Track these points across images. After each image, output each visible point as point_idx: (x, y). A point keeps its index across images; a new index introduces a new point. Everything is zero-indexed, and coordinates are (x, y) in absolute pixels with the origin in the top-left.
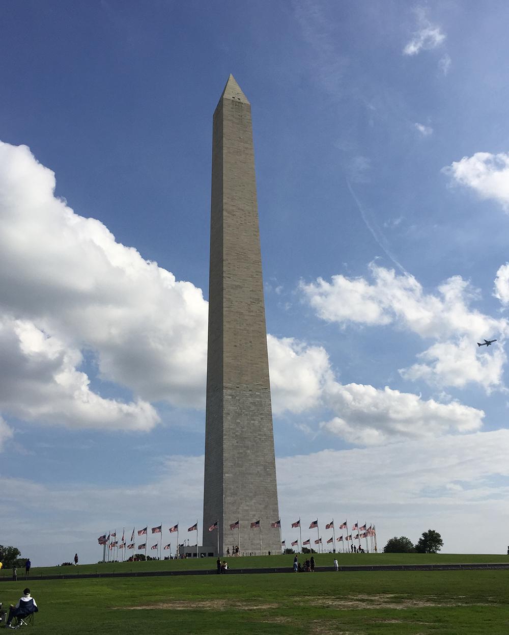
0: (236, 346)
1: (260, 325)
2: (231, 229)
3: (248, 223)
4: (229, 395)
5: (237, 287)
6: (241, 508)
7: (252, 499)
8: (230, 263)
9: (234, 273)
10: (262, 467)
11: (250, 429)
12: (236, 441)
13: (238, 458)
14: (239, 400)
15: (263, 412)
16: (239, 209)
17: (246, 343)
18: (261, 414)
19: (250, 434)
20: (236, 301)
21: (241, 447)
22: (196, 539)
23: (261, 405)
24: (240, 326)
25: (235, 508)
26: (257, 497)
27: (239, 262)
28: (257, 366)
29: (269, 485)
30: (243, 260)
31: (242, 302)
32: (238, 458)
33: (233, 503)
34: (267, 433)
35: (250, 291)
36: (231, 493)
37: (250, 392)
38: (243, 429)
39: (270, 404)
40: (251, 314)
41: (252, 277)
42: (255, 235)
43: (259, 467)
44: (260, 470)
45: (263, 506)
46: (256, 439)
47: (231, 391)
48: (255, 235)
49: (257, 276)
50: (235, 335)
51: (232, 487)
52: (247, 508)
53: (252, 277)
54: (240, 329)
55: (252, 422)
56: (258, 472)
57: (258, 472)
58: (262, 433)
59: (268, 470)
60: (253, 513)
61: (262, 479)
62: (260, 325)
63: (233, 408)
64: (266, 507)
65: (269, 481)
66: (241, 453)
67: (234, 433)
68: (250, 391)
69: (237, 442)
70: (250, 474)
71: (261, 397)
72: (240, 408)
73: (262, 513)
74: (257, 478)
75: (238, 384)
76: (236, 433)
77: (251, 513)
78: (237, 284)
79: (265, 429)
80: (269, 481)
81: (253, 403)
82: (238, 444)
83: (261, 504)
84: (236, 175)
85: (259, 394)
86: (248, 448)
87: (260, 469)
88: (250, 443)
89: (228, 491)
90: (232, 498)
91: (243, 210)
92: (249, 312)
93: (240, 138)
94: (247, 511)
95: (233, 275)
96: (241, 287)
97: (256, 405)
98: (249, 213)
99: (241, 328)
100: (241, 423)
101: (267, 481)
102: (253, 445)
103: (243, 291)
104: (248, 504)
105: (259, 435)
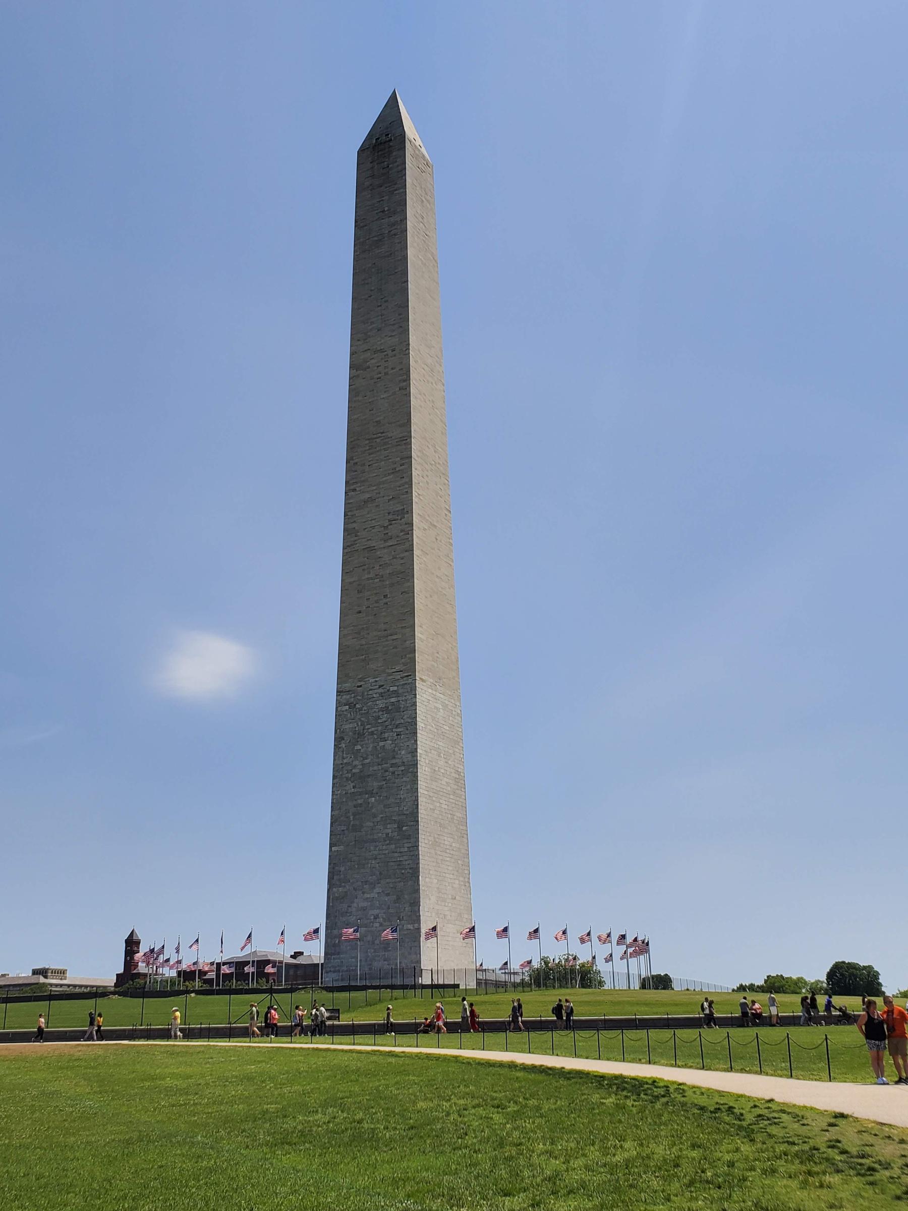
0: (360, 612)
1: (402, 559)
2: (360, 398)
6: (355, 905)
7: (374, 888)
11: (378, 757)
12: (352, 785)
14: (361, 709)
15: (402, 721)
16: (375, 352)
21: (361, 794)
23: (398, 710)
25: (345, 906)
28: (395, 637)
32: (354, 815)
34: (405, 760)
35: (389, 500)
37: (381, 690)
38: (367, 761)
39: (415, 704)
40: (390, 543)
41: (394, 471)
43: (389, 826)
47: (348, 697)
52: (365, 904)
55: (381, 744)
57: (387, 834)
58: (397, 761)
59: (404, 828)
60: (376, 912)
61: (393, 846)
62: (402, 559)
63: (351, 725)
64: (398, 898)
65: (406, 849)
68: (380, 686)
70: (374, 841)
73: (391, 911)
77: (371, 912)
78: (367, 496)
79: (403, 752)
80: (406, 849)
83: (388, 895)
86: (371, 794)
87: (390, 829)
88: (375, 784)
89: (335, 877)
91: (382, 351)
93: (383, 211)
94: (364, 909)
95: (363, 481)
96: (371, 500)
99: (371, 576)
101: (402, 850)
102: (381, 787)
104: (368, 896)
105: (392, 765)
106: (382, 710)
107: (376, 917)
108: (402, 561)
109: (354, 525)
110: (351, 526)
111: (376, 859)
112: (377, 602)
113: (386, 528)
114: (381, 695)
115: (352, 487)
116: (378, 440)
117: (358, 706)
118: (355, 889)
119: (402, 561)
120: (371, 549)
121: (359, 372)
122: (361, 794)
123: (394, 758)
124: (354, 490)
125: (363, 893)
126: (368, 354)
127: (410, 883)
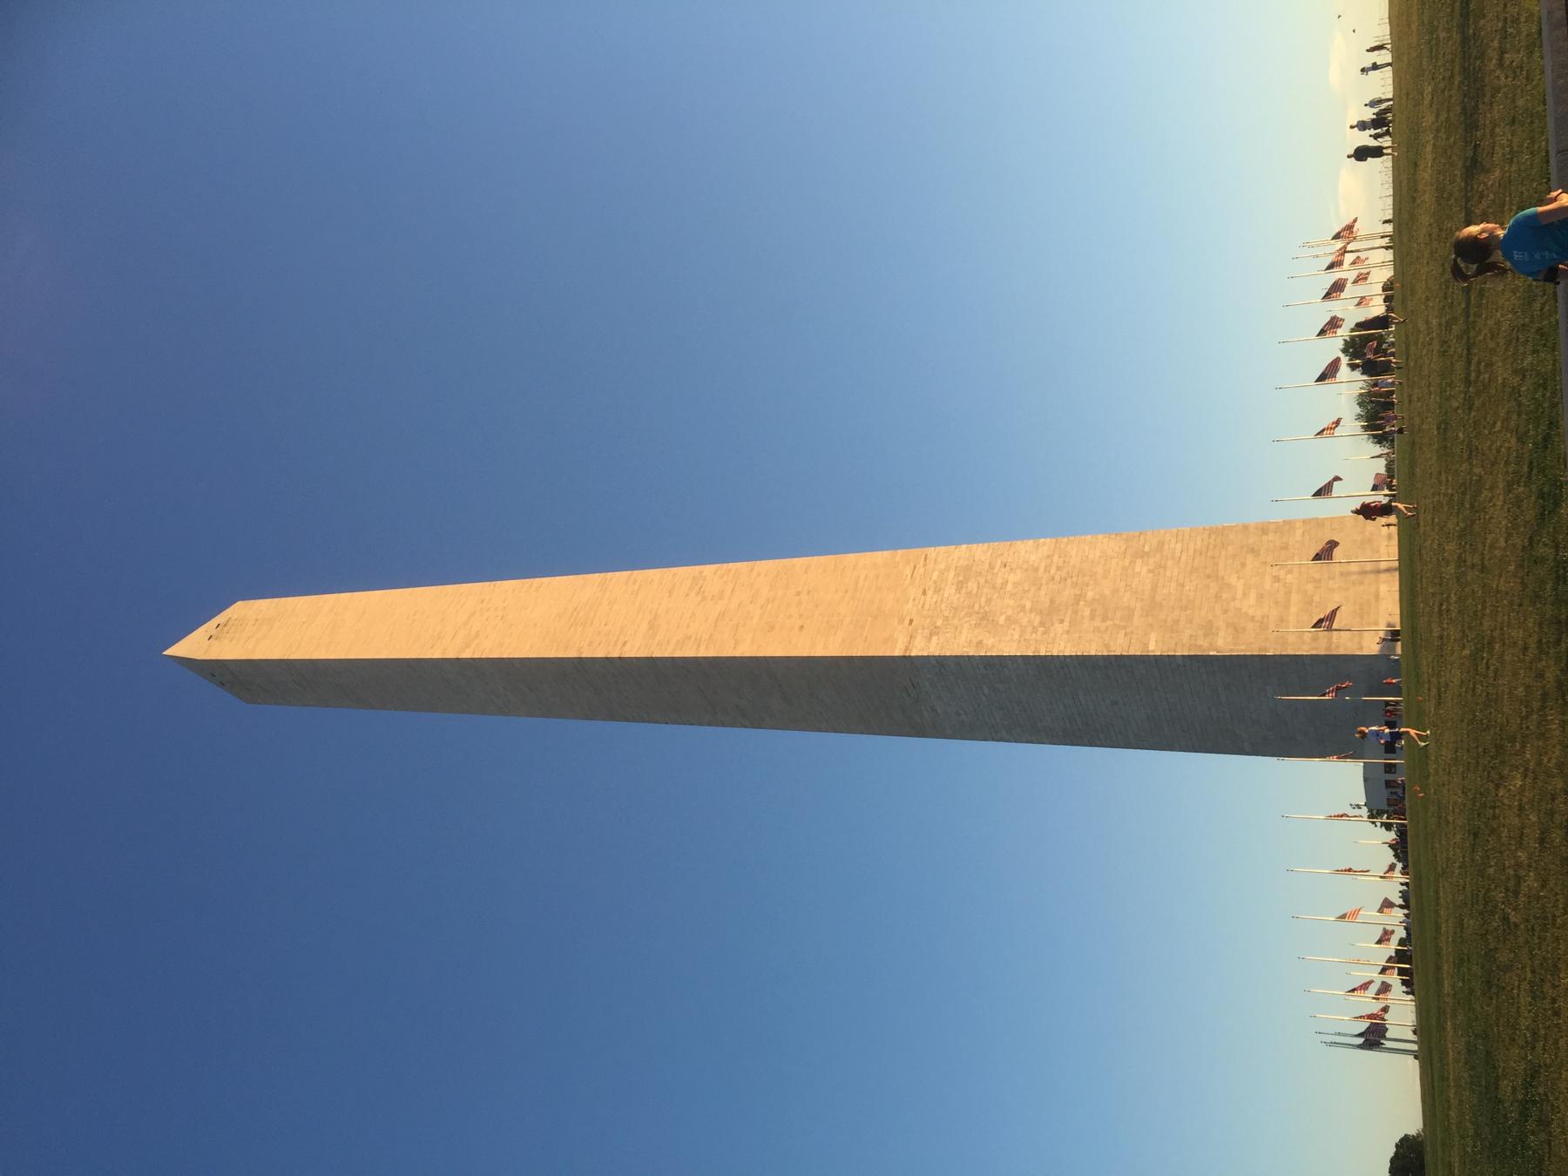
4: (930, 639)
5: (652, 626)
6: (1251, 612)
8: (591, 643)
10: (1139, 561)
12: (1057, 625)
13: (1103, 620)
17: (799, 604)
18: (991, 567)
19: (1042, 593)
21: (1075, 612)
22: (1342, 780)
23: (968, 568)
25: (1250, 625)
26: (1221, 573)
29: (1192, 546)
31: (693, 614)
32: (1103, 620)
33: (1237, 630)
36: (1206, 635)
37: (930, 593)
38: (1028, 605)
44: (1145, 569)
45: (1250, 559)
46: (1057, 578)
47: (919, 637)
50: (773, 628)
51: (1188, 632)
55: (1009, 587)
56: (1149, 571)
57: (1149, 571)
61: (1170, 563)
63: (965, 631)
64: (1254, 551)
66: (1093, 611)
67: (1035, 630)
68: (924, 593)
69: (1062, 621)
71: (947, 569)
72: (969, 615)
74: (1168, 574)
75: (901, 621)
76: (1036, 623)
81: (960, 586)
82: (1067, 620)
83: (1243, 565)
85: (936, 574)
89: (1200, 642)
90: (1222, 634)
92: (721, 598)
94: (1260, 597)
97: (966, 580)
100: (1009, 612)
104: (1240, 592)
106: (958, 590)
107: (1277, 579)
111: (1183, 585)
114: (937, 591)
117: (939, 623)
118: (1226, 611)
120: (722, 615)
122: (1075, 612)
123: (1036, 570)
125: (1234, 599)
127: (1231, 536)
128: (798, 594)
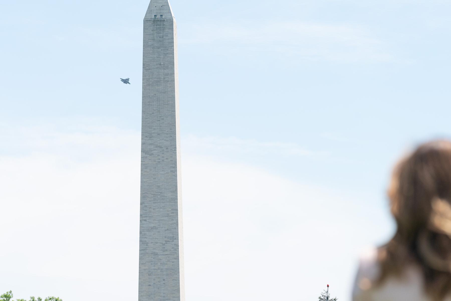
1: (173, 262)
3: (165, 160)
8: (146, 206)
9: (150, 215)
20: (152, 243)
24: (154, 266)
27: (155, 203)
30: (159, 201)
35: (165, 230)
42: (171, 171)
48: (171, 171)
49: (172, 214)
50: (149, 275)
53: (168, 216)
54: (154, 269)
78: (152, 225)
84: (155, 109)
91: (160, 147)
93: (160, 64)
95: (150, 217)
98: (167, 149)
103: (159, 232)
108: (173, 264)
109: (145, 239)
110: (143, 239)
112: (159, 282)
113: (164, 244)
115: (144, 219)
116: (159, 196)
119: (173, 264)
121: (147, 155)
124: (145, 220)
126: (152, 147)
128: (164, 280)
